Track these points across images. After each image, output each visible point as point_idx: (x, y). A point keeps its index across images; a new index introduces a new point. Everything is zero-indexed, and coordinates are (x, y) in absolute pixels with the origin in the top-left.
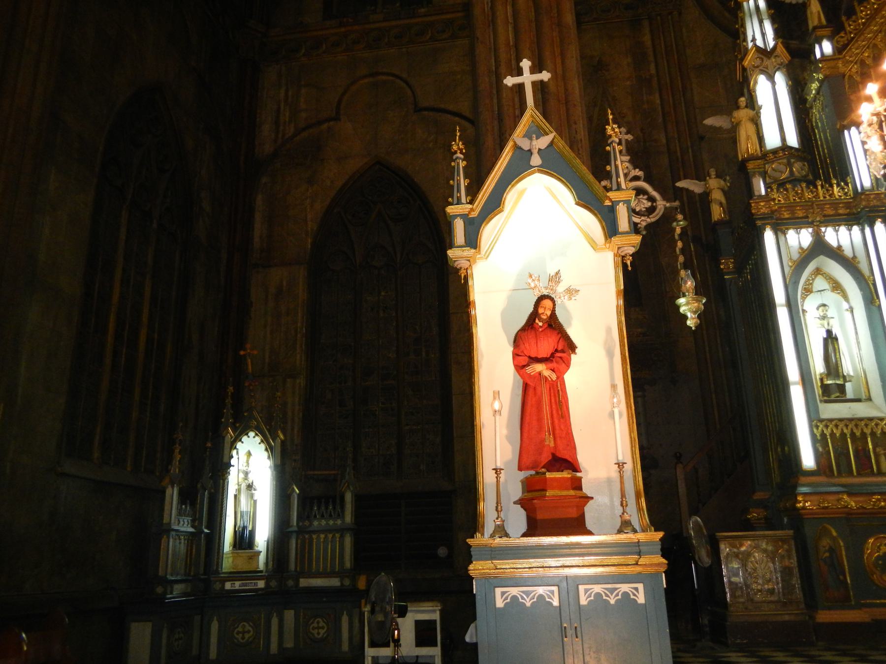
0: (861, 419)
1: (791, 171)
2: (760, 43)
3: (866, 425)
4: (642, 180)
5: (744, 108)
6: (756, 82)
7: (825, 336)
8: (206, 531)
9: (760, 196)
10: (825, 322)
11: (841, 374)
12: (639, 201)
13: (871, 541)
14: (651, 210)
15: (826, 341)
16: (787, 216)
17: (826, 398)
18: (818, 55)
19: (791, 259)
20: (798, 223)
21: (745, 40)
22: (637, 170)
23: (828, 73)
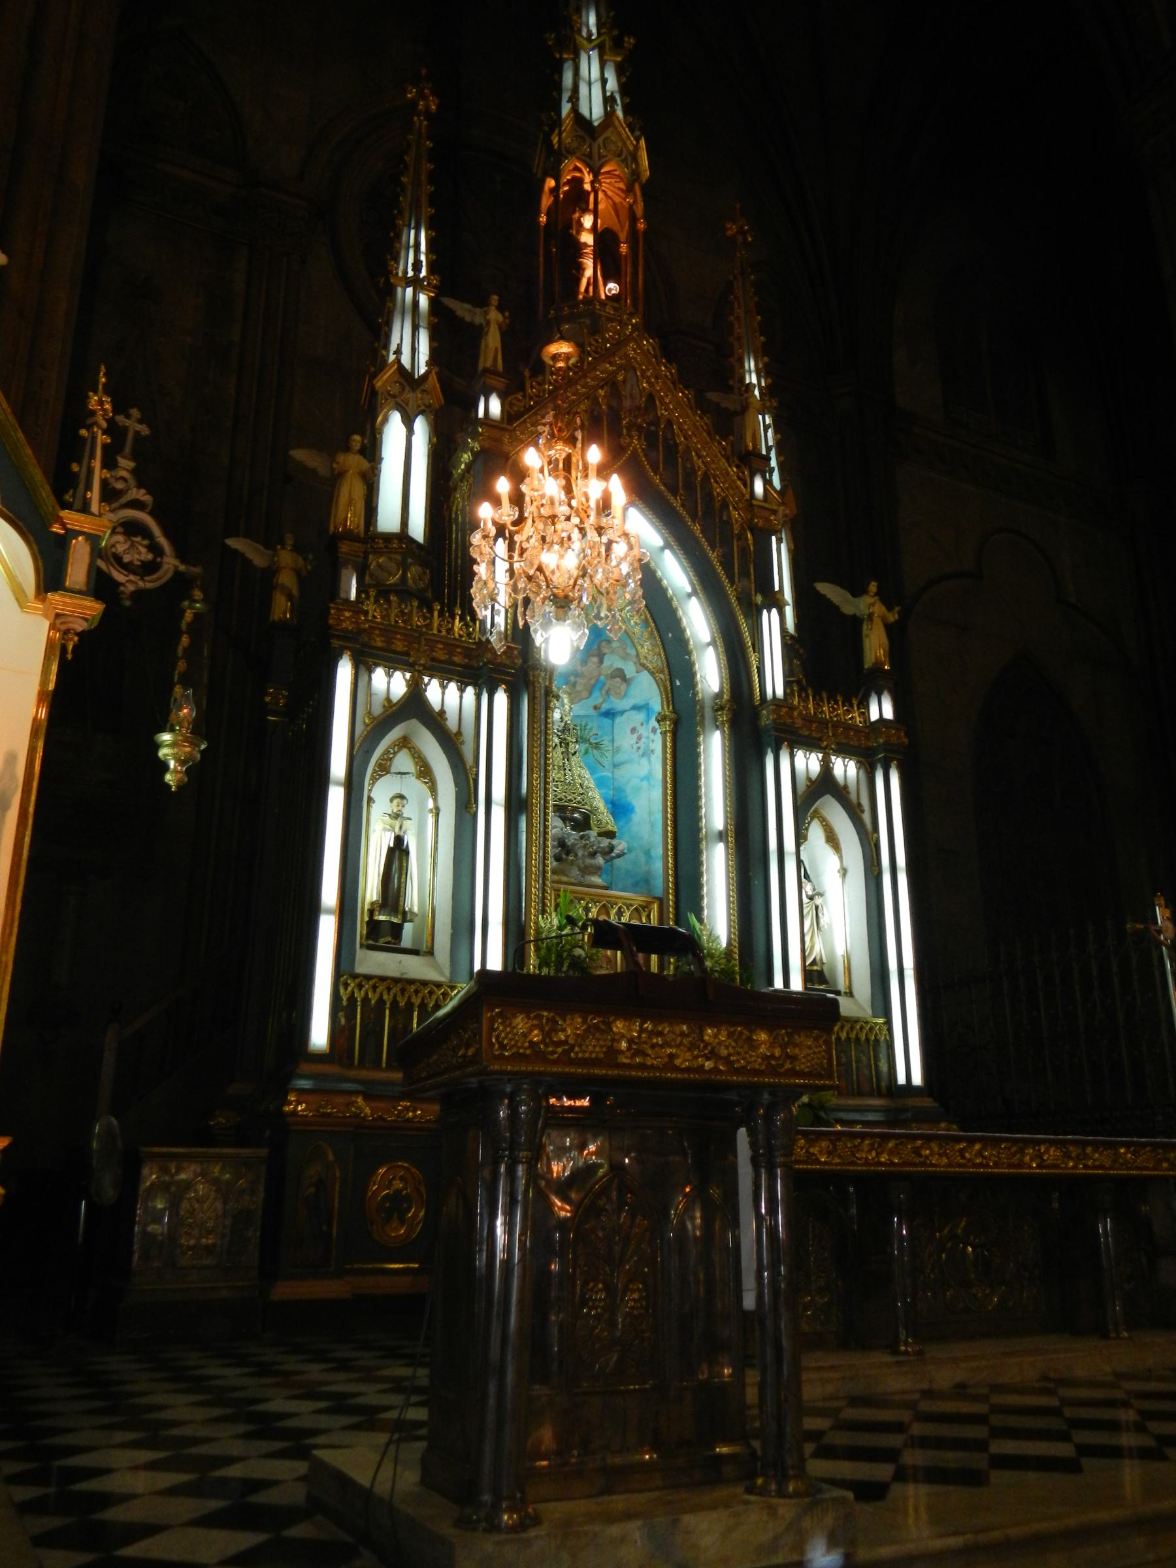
0: (411, 982)
1: (404, 575)
2: (406, 360)
3: (417, 992)
4: (148, 511)
5: (355, 453)
6: (386, 420)
7: (392, 845)
9: (347, 600)
10: (397, 824)
11: (401, 908)
12: (132, 545)
13: (382, 1171)
14: (148, 568)
15: (391, 851)
16: (380, 644)
17: (371, 942)
18: (481, 414)
19: (370, 713)
21: (386, 346)
22: (143, 491)
23: (486, 445)
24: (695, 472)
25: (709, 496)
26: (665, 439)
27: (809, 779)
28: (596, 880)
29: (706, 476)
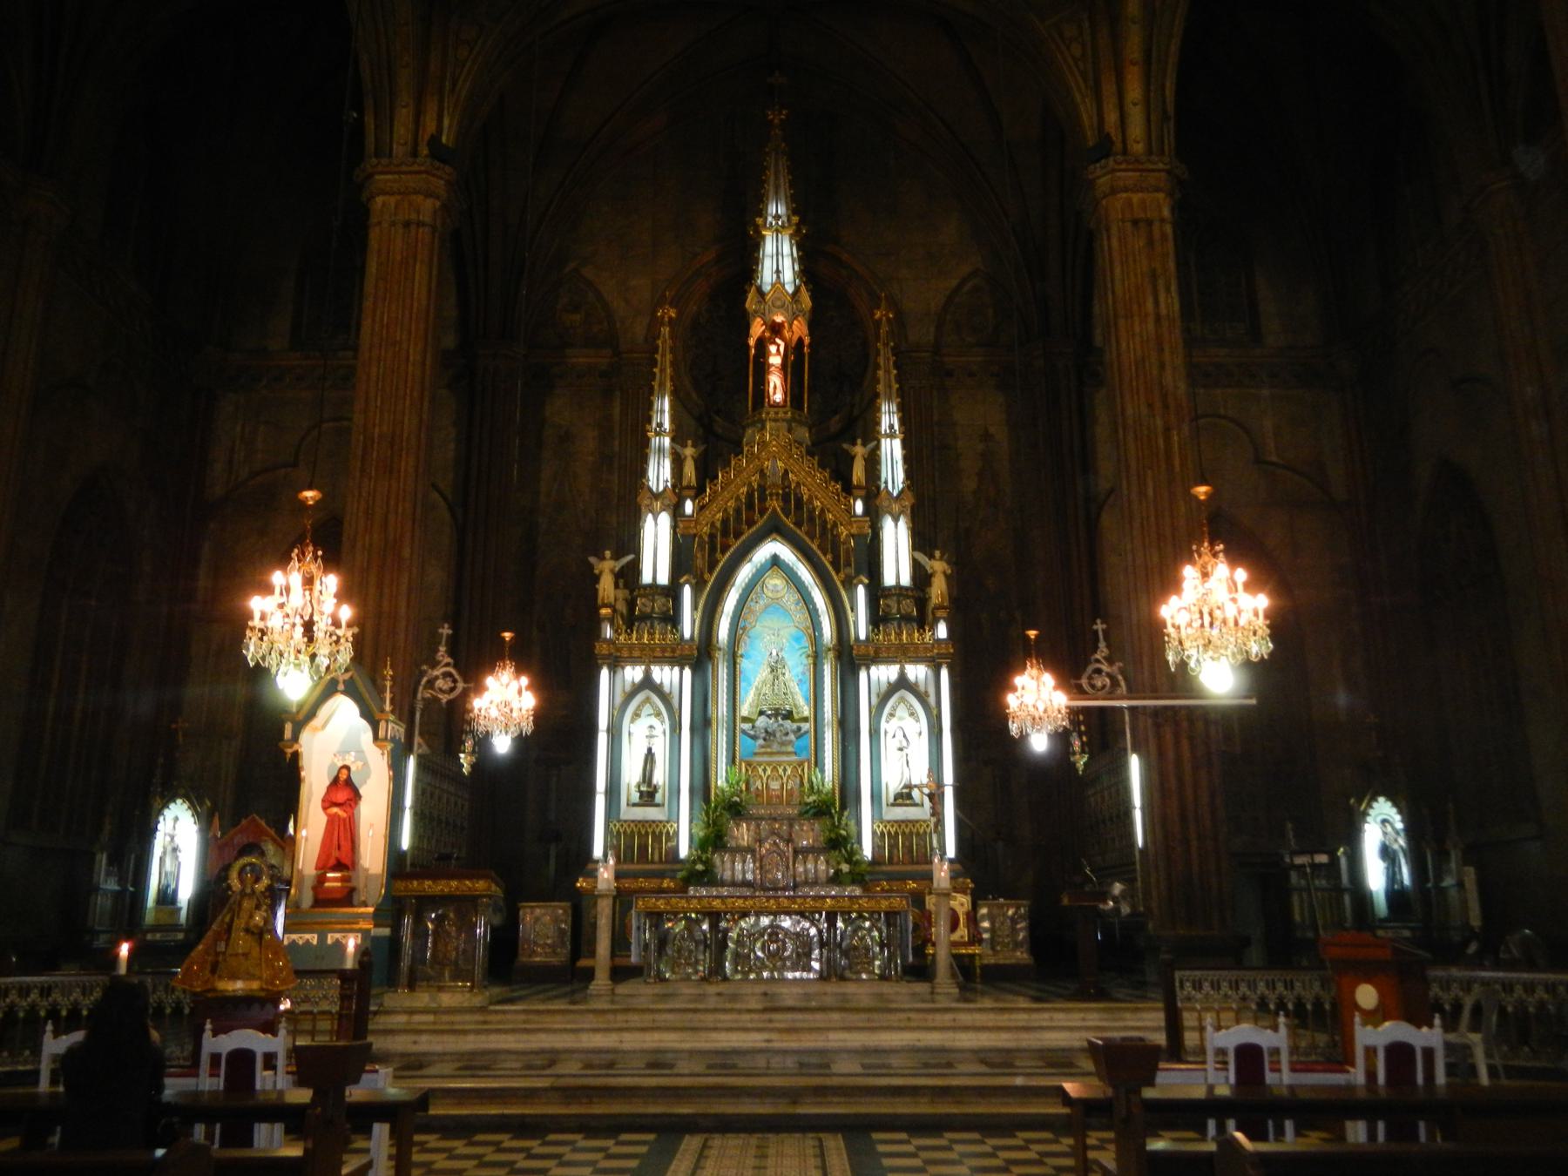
0: (647, 822)
1: (653, 607)
8: (131, 889)
20: (634, 661)
24: (814, 509)
25: (825, 522)
26: (795, 494)
27: (889, 683)
28: (790, 749)
29: (822, 511)
